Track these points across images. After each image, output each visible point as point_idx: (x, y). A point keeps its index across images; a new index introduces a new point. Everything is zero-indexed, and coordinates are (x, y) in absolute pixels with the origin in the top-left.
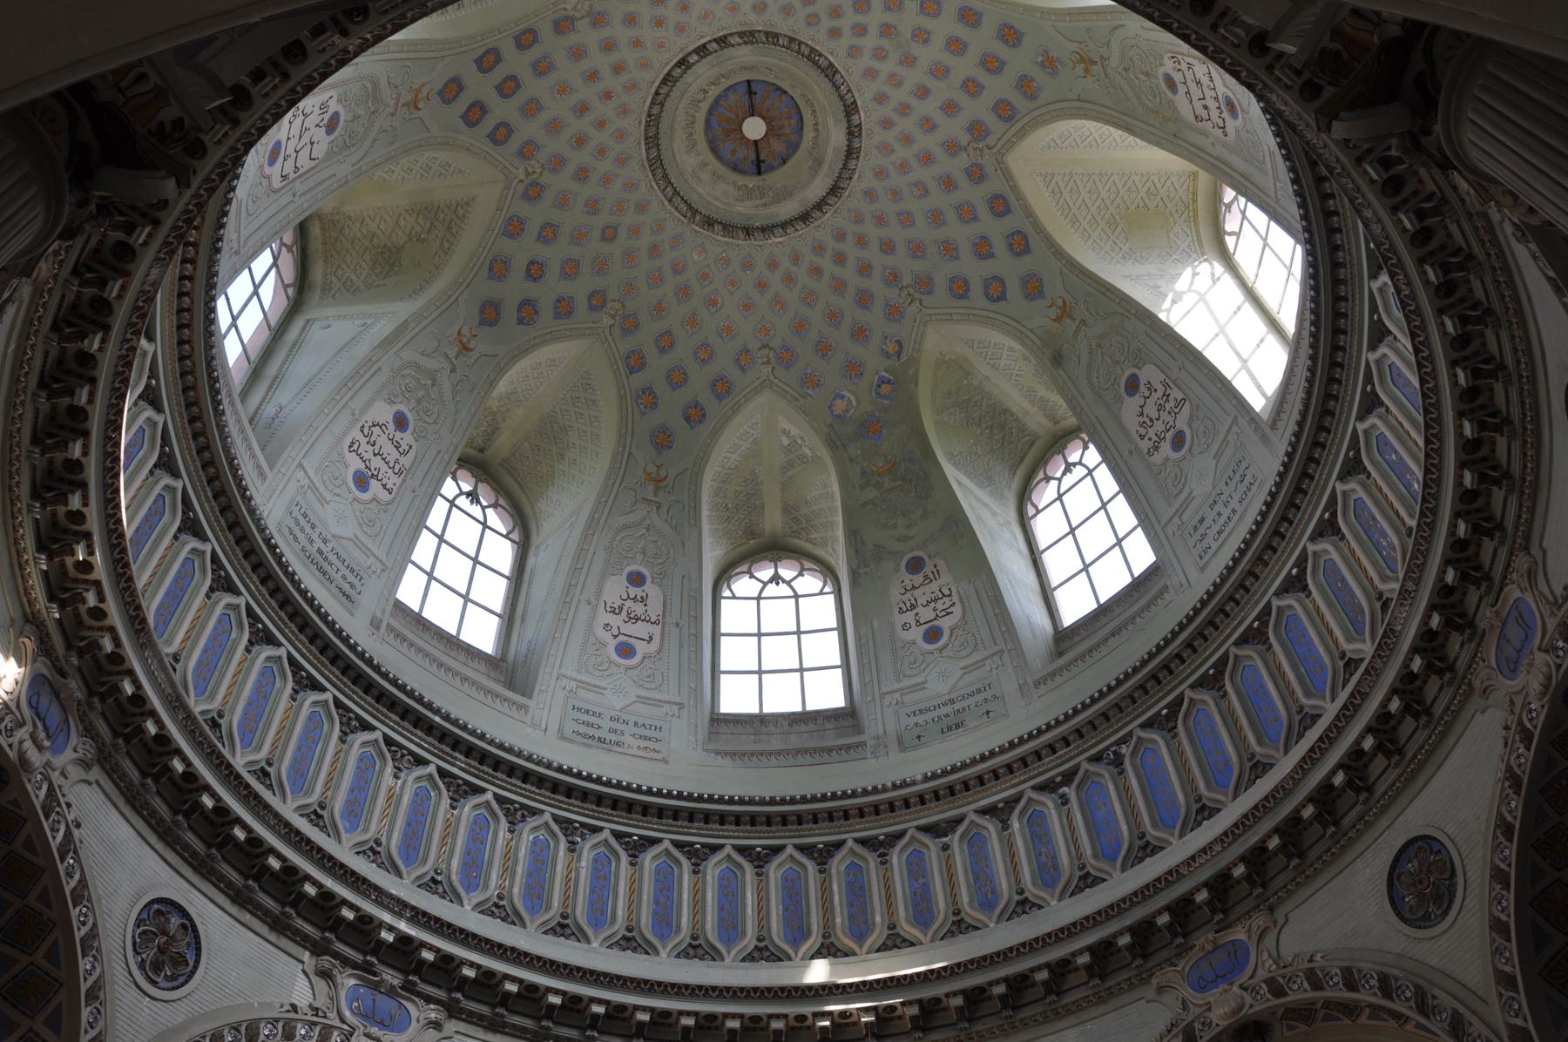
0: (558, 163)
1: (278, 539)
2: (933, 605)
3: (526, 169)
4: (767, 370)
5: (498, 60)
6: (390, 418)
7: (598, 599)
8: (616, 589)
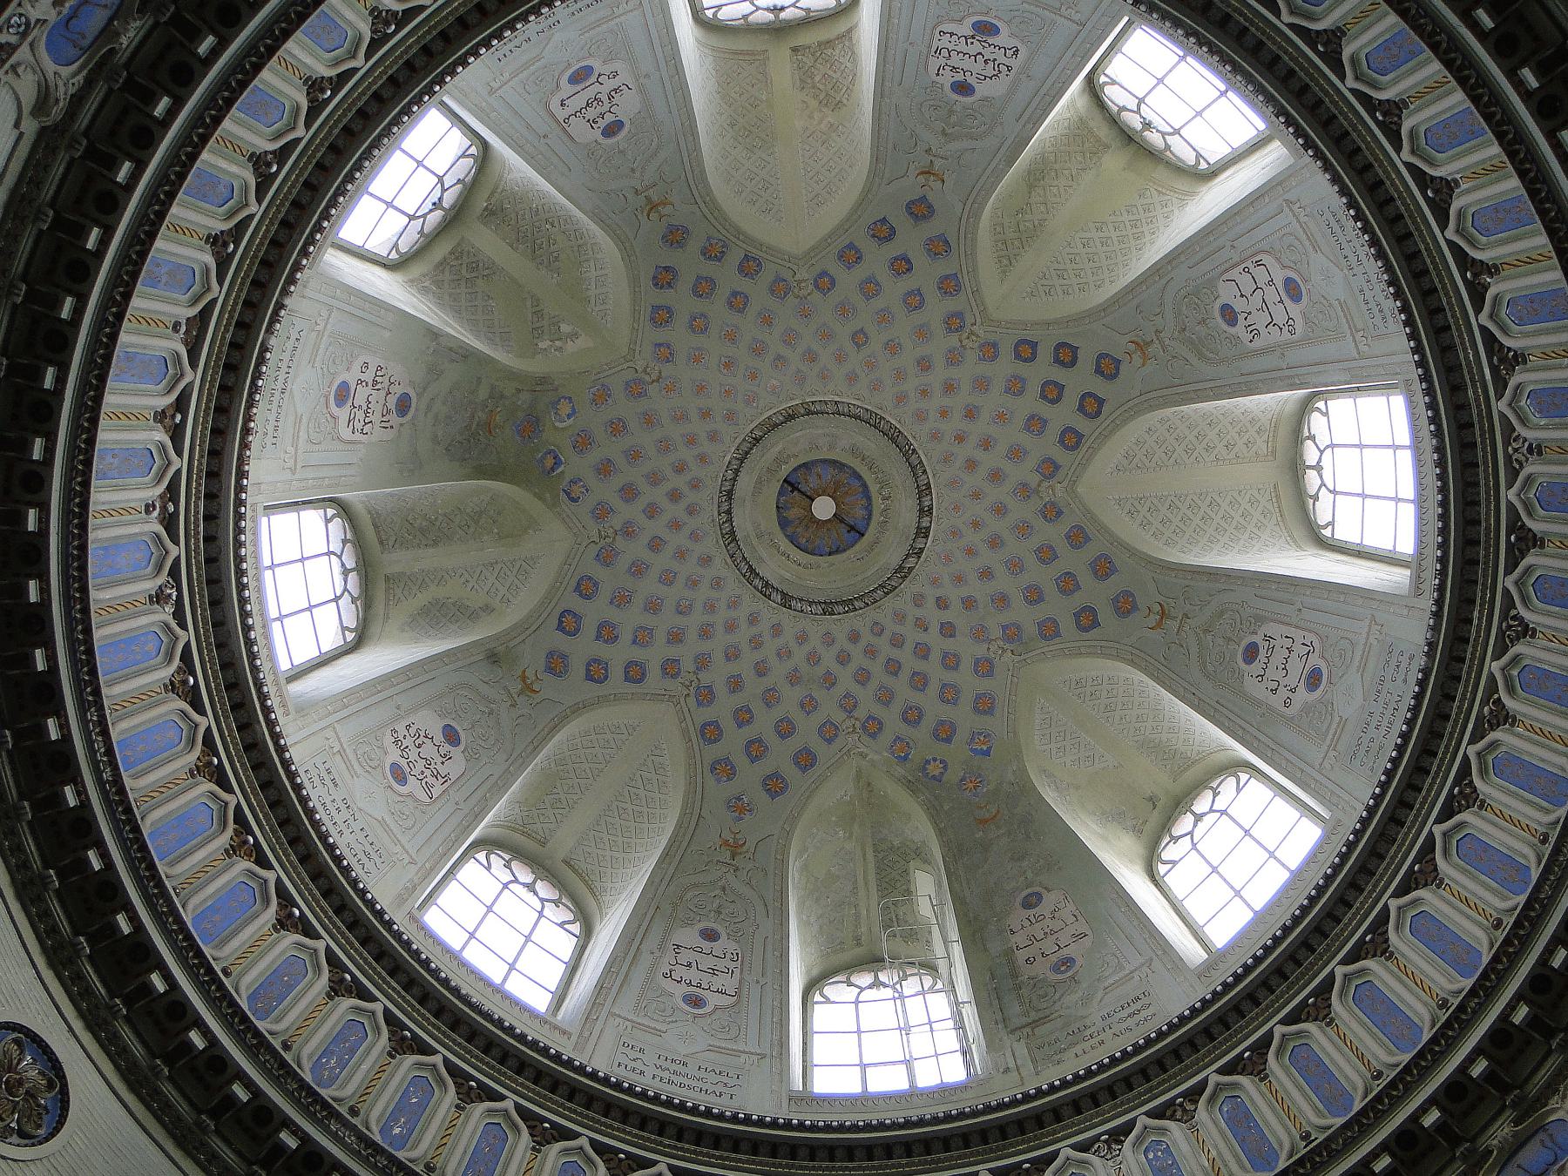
0: (953, 359)
2: (365, 408)
3: (978, 336)
4: (640, 366)
6: (976, 86)
8: (627, 107)
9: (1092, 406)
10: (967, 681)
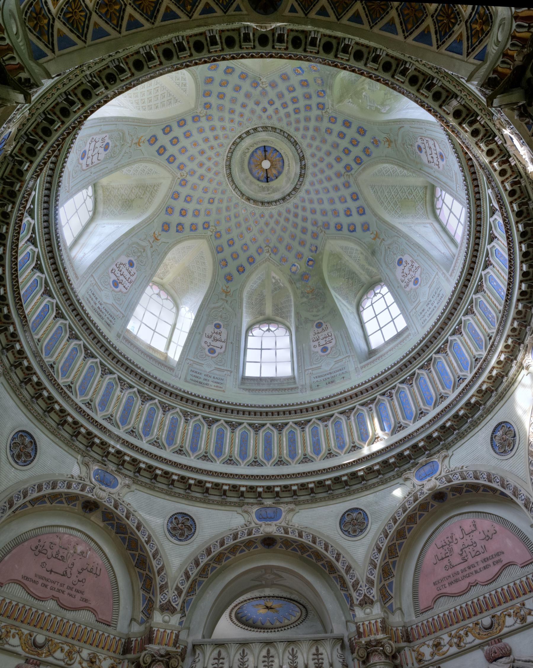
0: (192, 173)
1: (82, 300)
4: (268, 255)
5: (171, 130)
6: (127, 262)
7: (203, 332)
8: (210, 329)
9: (167, 130)
10: (282, 87)
